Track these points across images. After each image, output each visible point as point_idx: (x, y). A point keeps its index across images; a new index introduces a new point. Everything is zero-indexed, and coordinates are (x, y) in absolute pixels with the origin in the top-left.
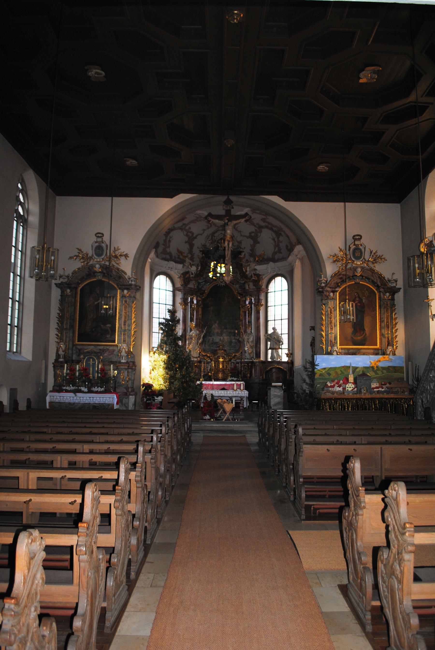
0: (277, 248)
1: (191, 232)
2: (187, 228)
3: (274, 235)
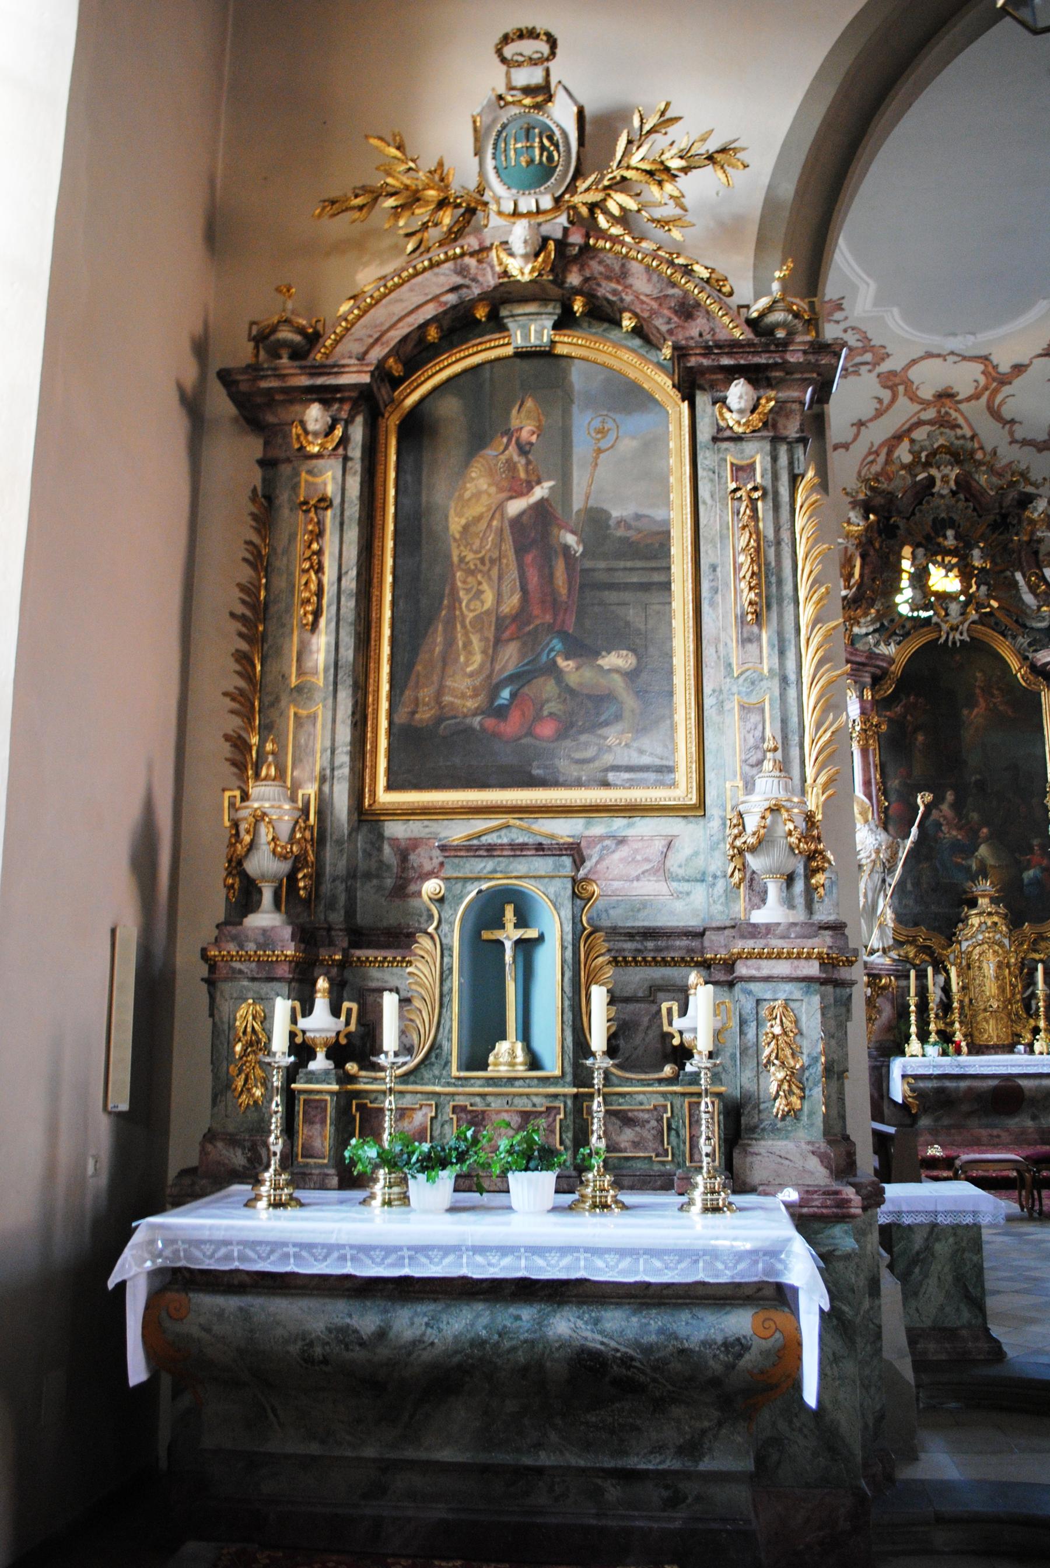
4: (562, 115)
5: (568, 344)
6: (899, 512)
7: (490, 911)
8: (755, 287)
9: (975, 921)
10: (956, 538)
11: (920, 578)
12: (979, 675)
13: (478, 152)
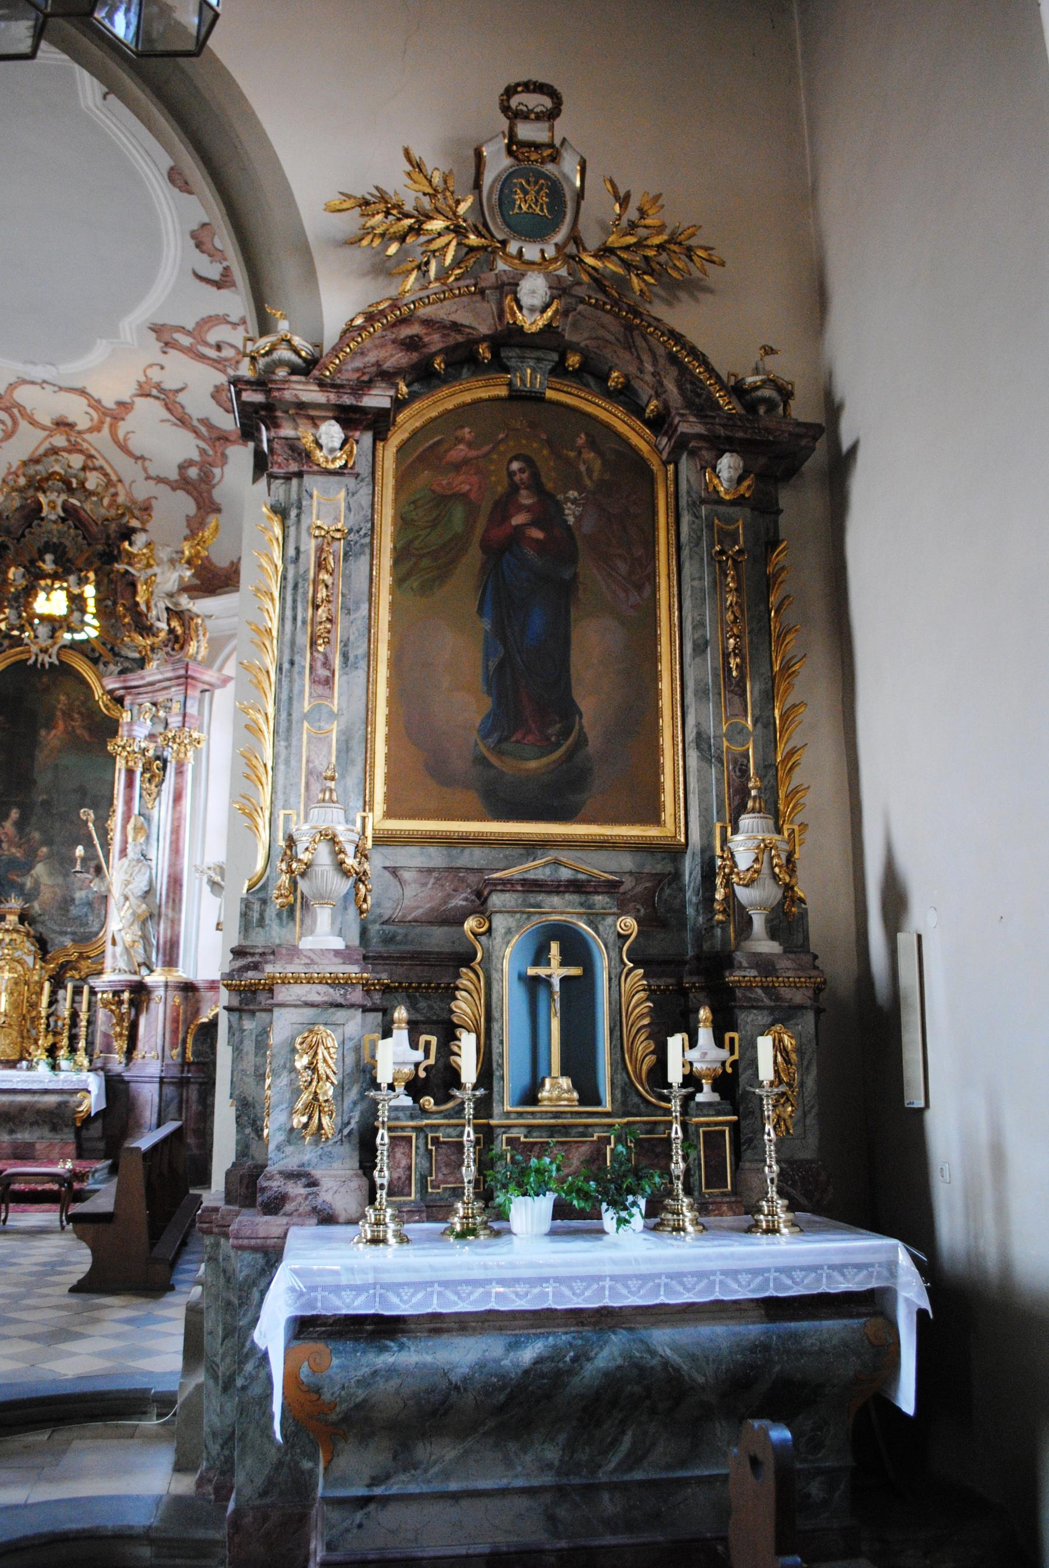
10: (55, 562)
12: (62, 698)
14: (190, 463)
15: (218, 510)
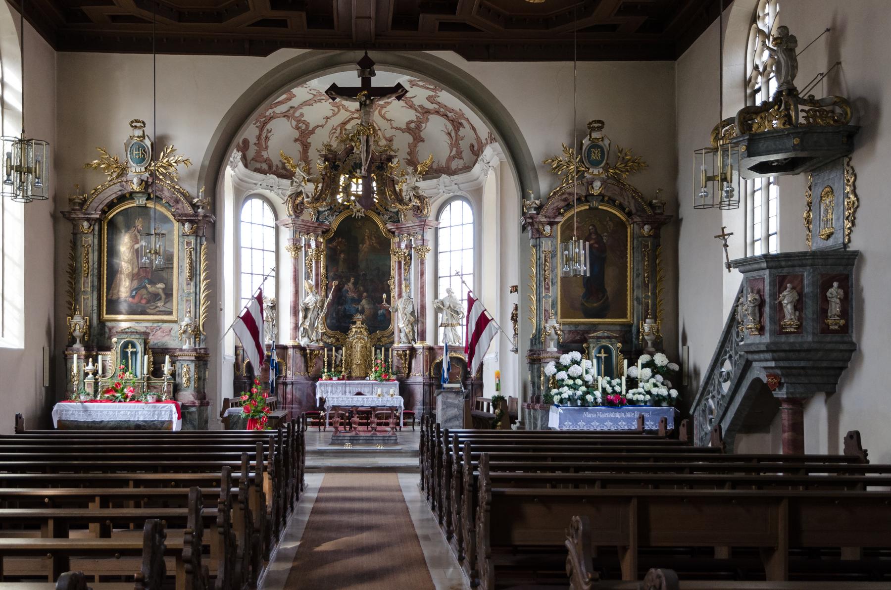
0: (455, 149)
1: (304, 122)
2: (297, 114)
3: (450, 127)
4: (148, 143)
5: (150, 205)
6: (339, 160)
7: (125, 346)
8: (196, 190)
9: (354, 330)
11: (347, 187)
13: (126, 151)
14: (412, 122)
15: (423, 141)
